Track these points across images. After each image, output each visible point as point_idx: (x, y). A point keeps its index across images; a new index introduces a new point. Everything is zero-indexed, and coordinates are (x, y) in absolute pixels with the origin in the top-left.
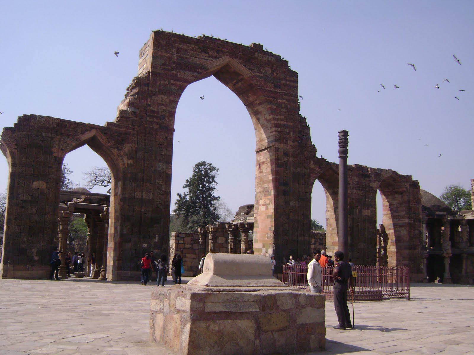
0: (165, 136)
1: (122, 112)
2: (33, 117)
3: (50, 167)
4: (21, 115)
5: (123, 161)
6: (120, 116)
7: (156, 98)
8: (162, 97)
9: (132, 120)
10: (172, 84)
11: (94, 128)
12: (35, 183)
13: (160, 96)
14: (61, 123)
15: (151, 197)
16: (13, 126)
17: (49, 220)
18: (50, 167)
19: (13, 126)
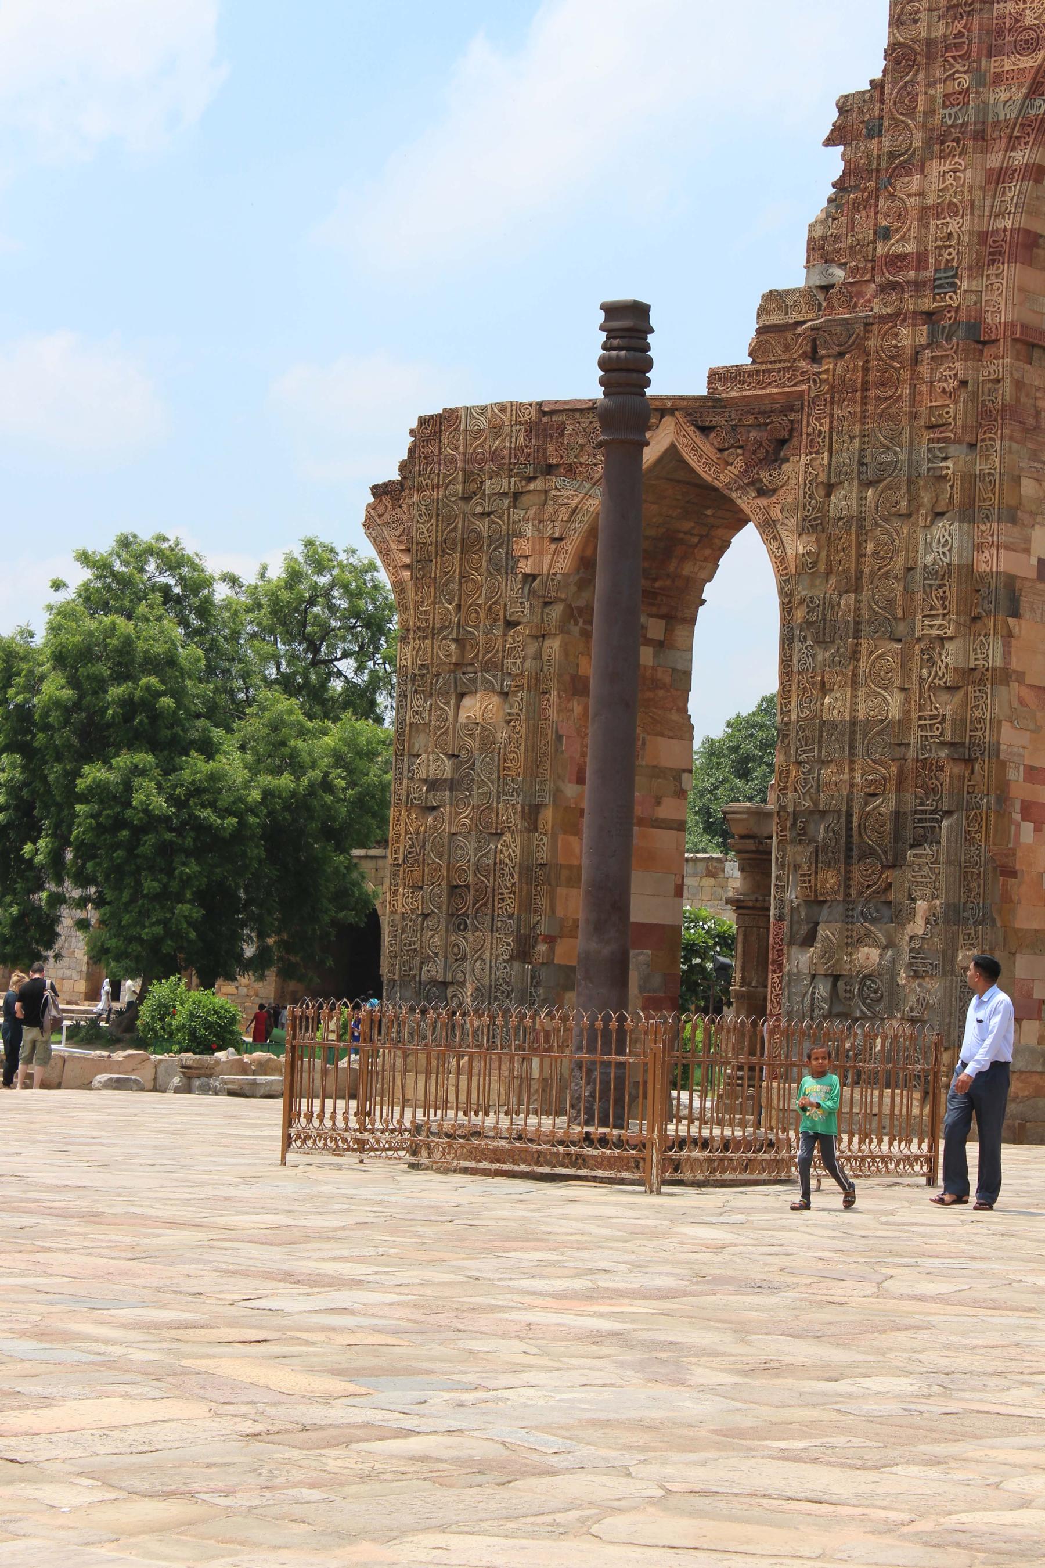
0: (955, 375)
1: (774, 300)
2: (449, 417)
3: (510, 624)
4: (414, 425)
5: (782, 546)
6: (760, 331)
7: (915, 182)
8: (942, 169)
9: (809, 333)
10: (998, 79)
11: (671, 411)
12: (467, 702)
13: (935, 167)
14: (545, 419)
15: (894, 705)
16: (396, 476)
17: (510, 854)
18: (510, 624)
19: (396, 476)
